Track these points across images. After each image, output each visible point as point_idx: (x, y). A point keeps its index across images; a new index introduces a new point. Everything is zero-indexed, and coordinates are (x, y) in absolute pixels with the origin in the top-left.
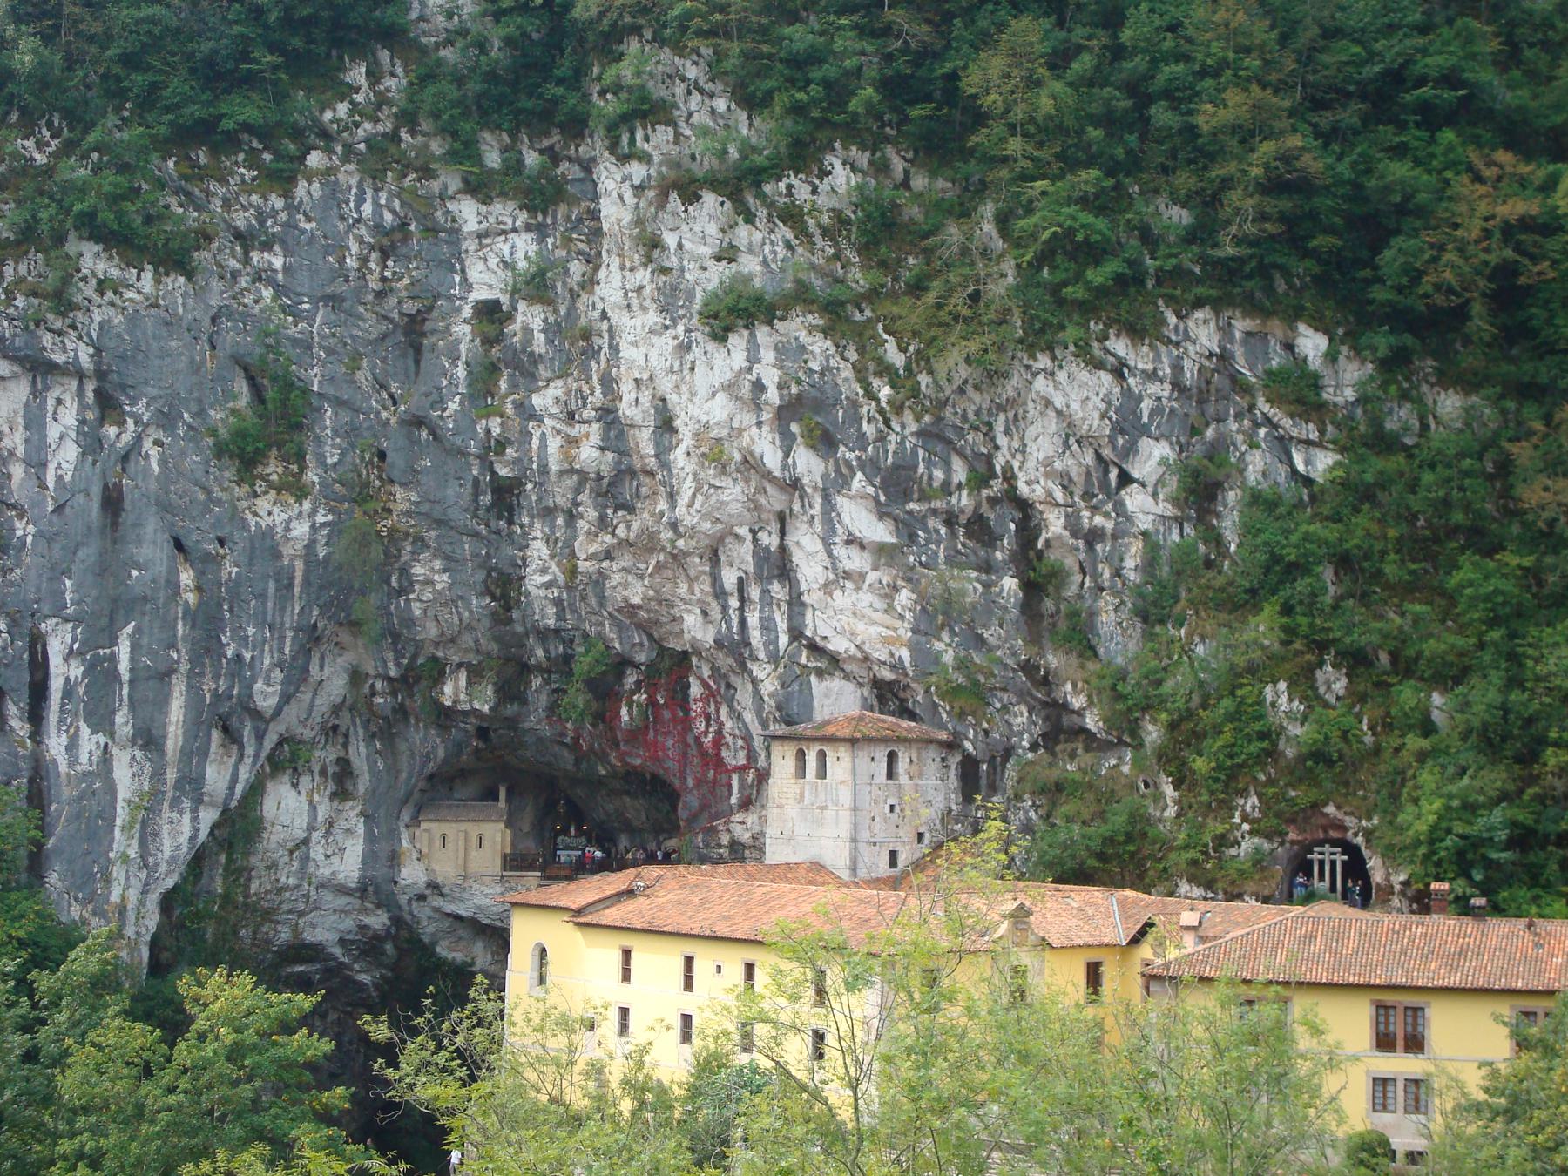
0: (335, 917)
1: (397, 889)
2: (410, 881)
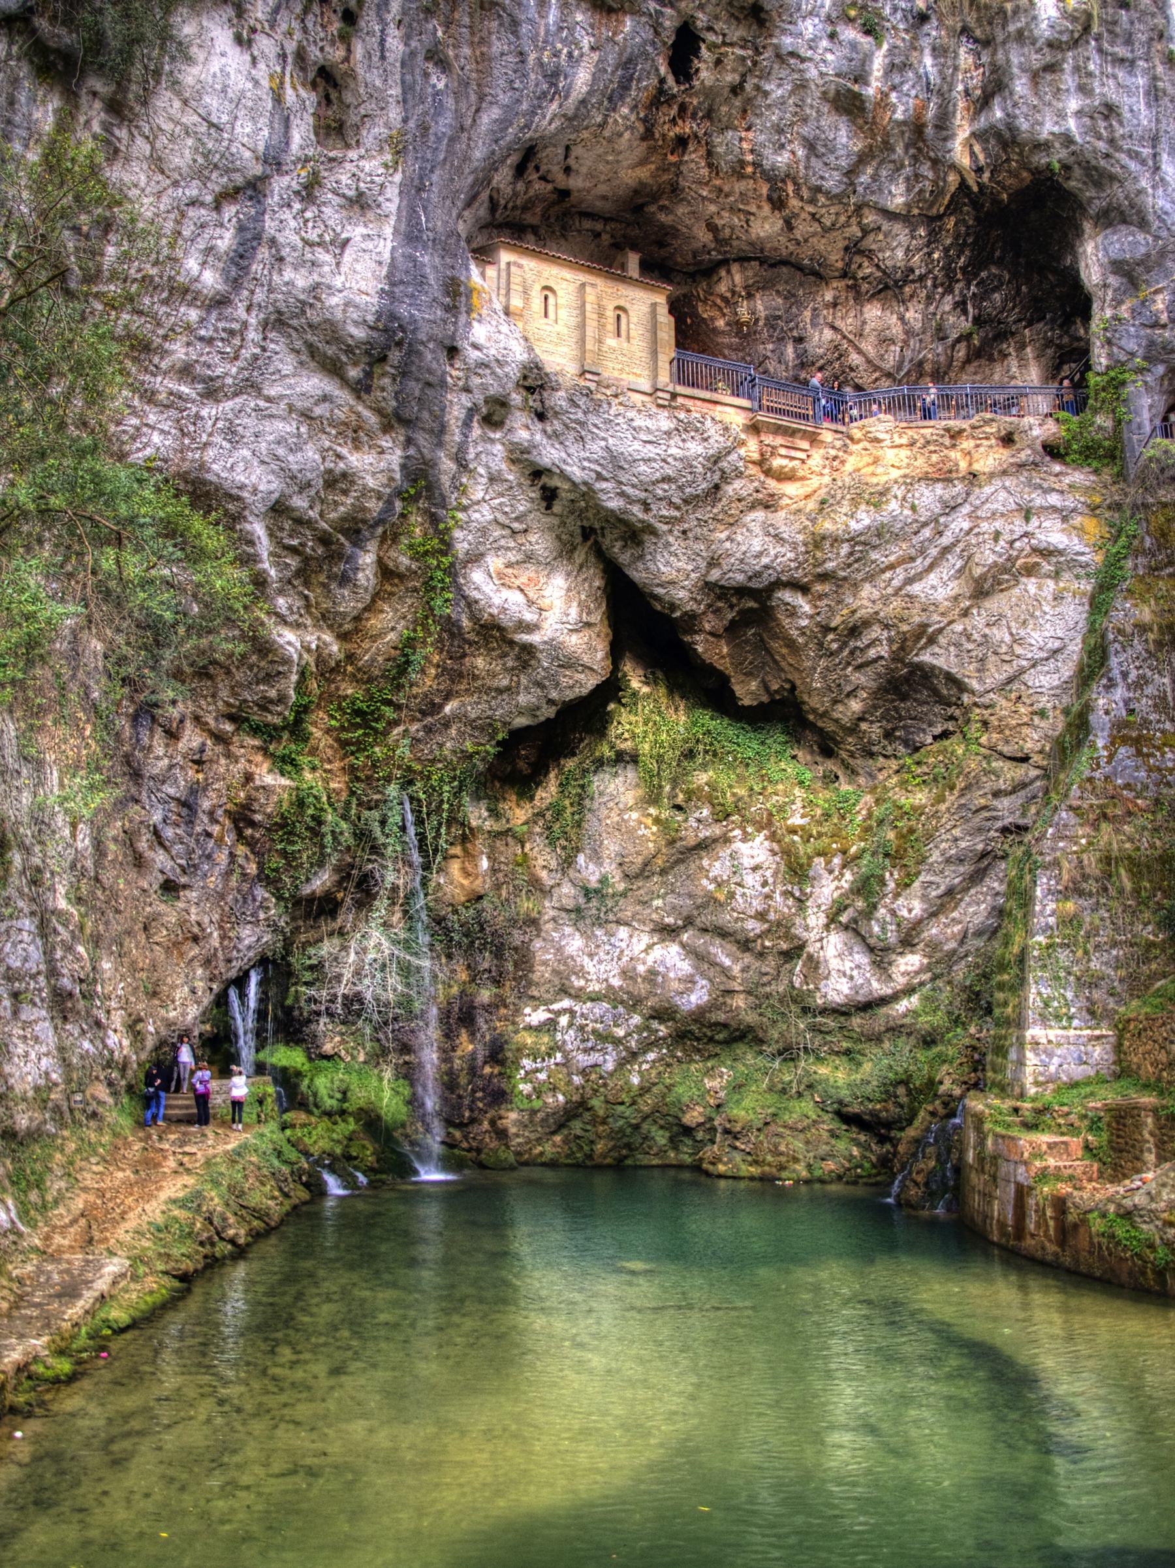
0: (290, 428)
1: (454, 373)
2: (493, 352)
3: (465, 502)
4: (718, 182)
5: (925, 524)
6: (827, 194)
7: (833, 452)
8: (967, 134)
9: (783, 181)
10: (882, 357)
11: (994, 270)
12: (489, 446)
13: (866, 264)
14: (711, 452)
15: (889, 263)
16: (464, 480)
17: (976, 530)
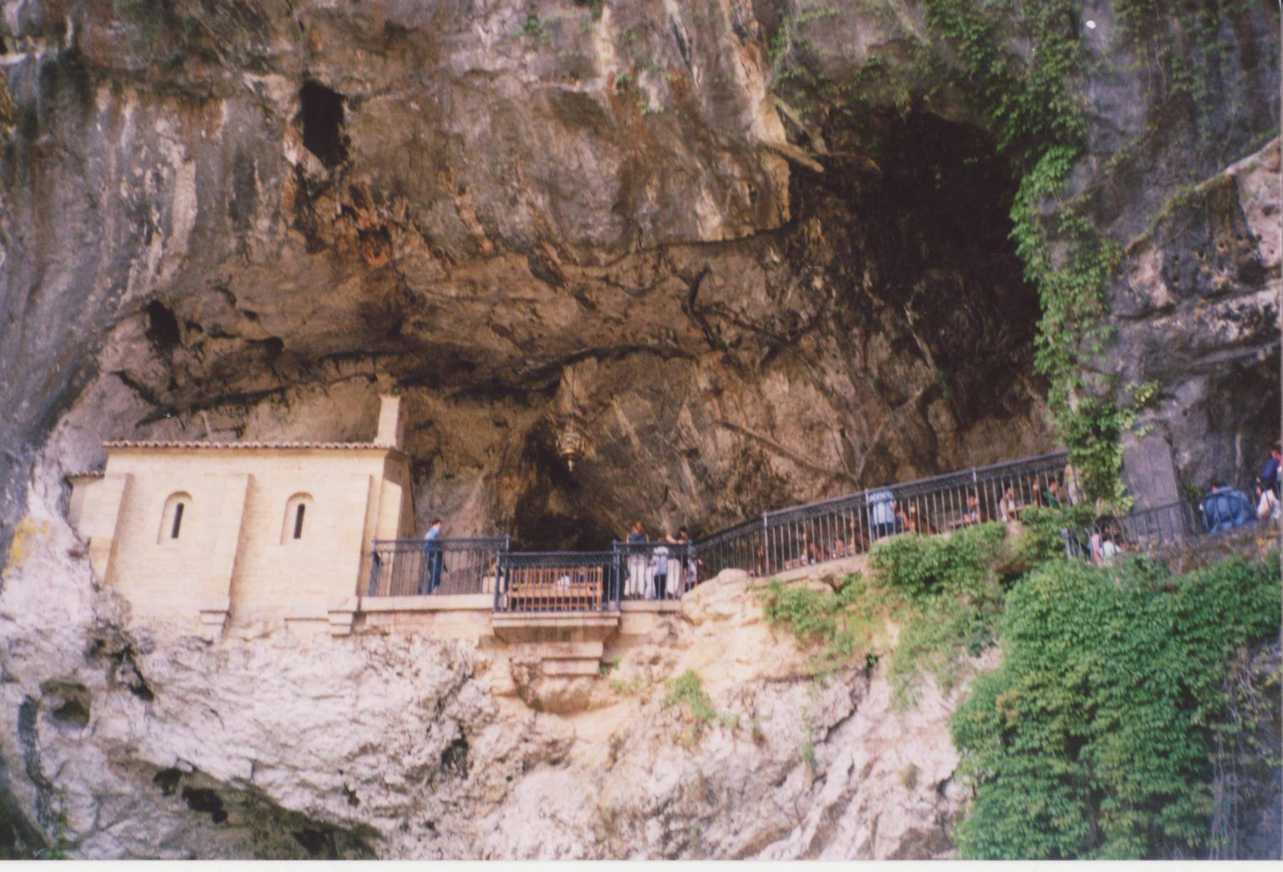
3: (70, 837)
4: (462, 273)
5: (790, 766)
6: (601, 245)
7: (649, 651)
8: (762, 94)
9: (540, 246)
10: (818, 453)
11: (935, 275)
12: (74, 751)
13: (724, 325)
14: (424, 694)
15: (753, 314)
16: (56, 806)
17: (875, 771)
